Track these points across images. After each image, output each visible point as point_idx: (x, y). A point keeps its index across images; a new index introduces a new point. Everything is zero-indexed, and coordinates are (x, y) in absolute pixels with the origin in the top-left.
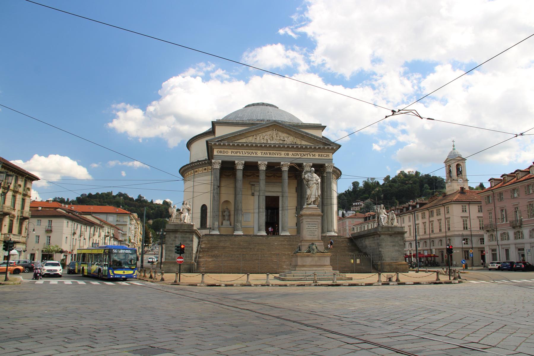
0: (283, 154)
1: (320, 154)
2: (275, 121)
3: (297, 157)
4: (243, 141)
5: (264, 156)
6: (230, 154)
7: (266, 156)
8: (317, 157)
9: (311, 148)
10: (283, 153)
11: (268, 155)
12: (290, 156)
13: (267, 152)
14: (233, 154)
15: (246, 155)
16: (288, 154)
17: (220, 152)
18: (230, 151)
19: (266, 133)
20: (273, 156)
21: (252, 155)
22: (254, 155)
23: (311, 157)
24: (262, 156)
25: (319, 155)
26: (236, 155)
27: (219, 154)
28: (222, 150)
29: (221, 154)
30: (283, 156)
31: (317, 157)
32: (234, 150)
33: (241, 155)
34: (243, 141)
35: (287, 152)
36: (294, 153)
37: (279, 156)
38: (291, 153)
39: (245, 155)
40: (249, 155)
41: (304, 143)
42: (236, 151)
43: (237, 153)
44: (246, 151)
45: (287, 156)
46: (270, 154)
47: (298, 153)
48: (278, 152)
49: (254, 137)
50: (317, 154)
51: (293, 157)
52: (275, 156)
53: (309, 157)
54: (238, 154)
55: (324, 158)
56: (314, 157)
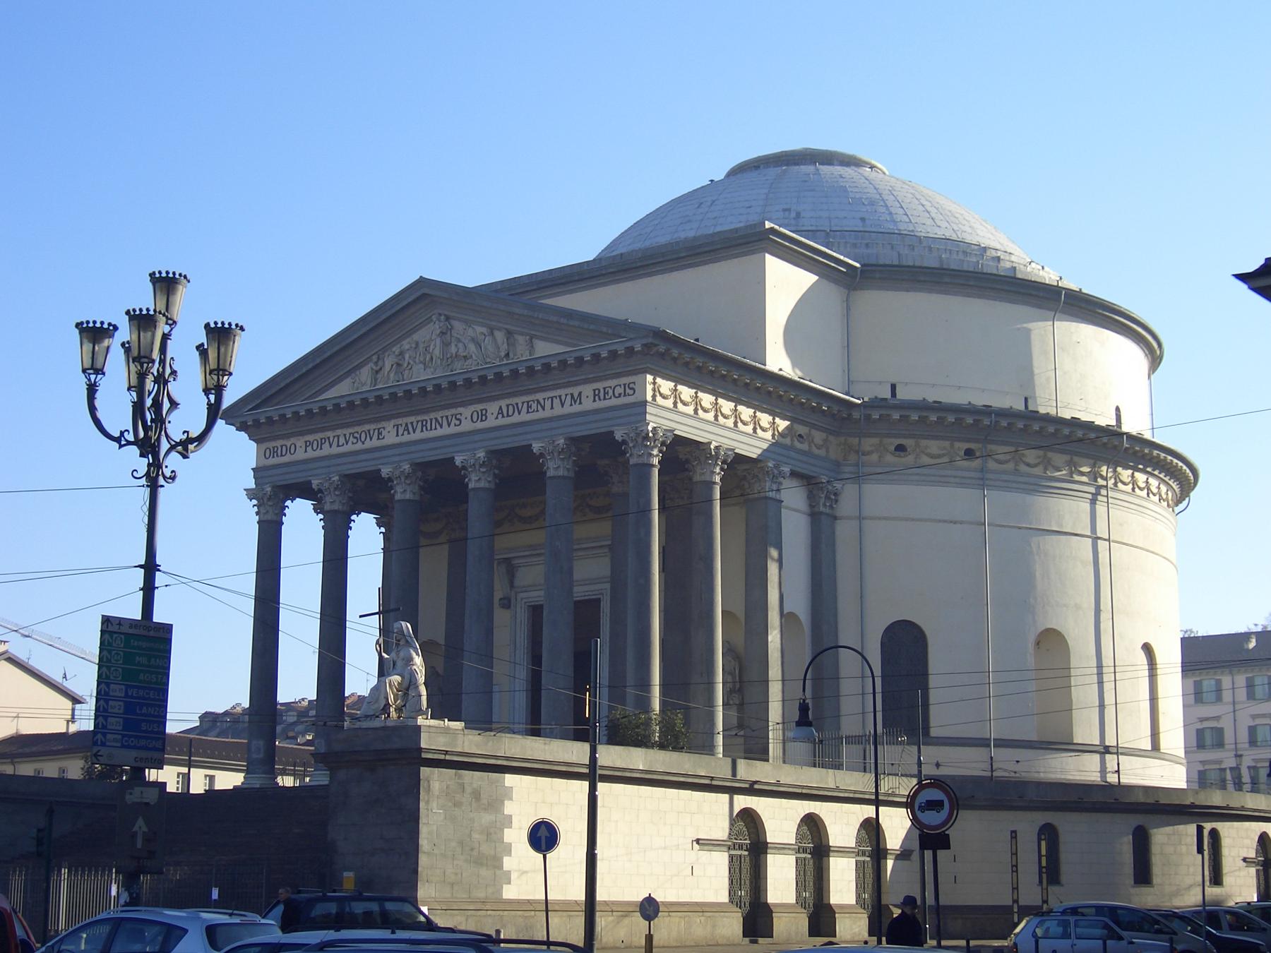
0: (466, 420)
1: (600, 385)
2: (422, 281)
3: (516, 418)
4: (343, 389)
5: (406, 438)
6: (300, 455)
8: (583, 402)
9: (596, 357)
10: (466, 412)
11: (418, 435)
12: (491, 422)
13: (412, 419)
14: (311, 454)
16: (483, 416)
17: (274, 452)
18: (300, 442)
19: (416, 337)
21: (368, 444)
22: (375, 443)
23: (568, 409)
25: (596, 395)
26: (318, 453)
27: (272, 461)
28: (278, 443)
30: (467, 426)
31: (588, 404)
32: (310, 438)
33: (335, 450)
34: (343, 389)
35: (479, 407)
36: (503, 403)
37: (453, 430)
38: (492, 408)
40: (359, 446)
41: (544, 349)
42: (319, 436)
44: (347, 431)
45: (480, 425)
47: (519, 400)
48: (449, 413)
49: (371, 365)
50: (587, 390)
51: (502, 421)
52: (440, 432)
53: (558, 410)
54: (326, 450)
56: (577, 408)
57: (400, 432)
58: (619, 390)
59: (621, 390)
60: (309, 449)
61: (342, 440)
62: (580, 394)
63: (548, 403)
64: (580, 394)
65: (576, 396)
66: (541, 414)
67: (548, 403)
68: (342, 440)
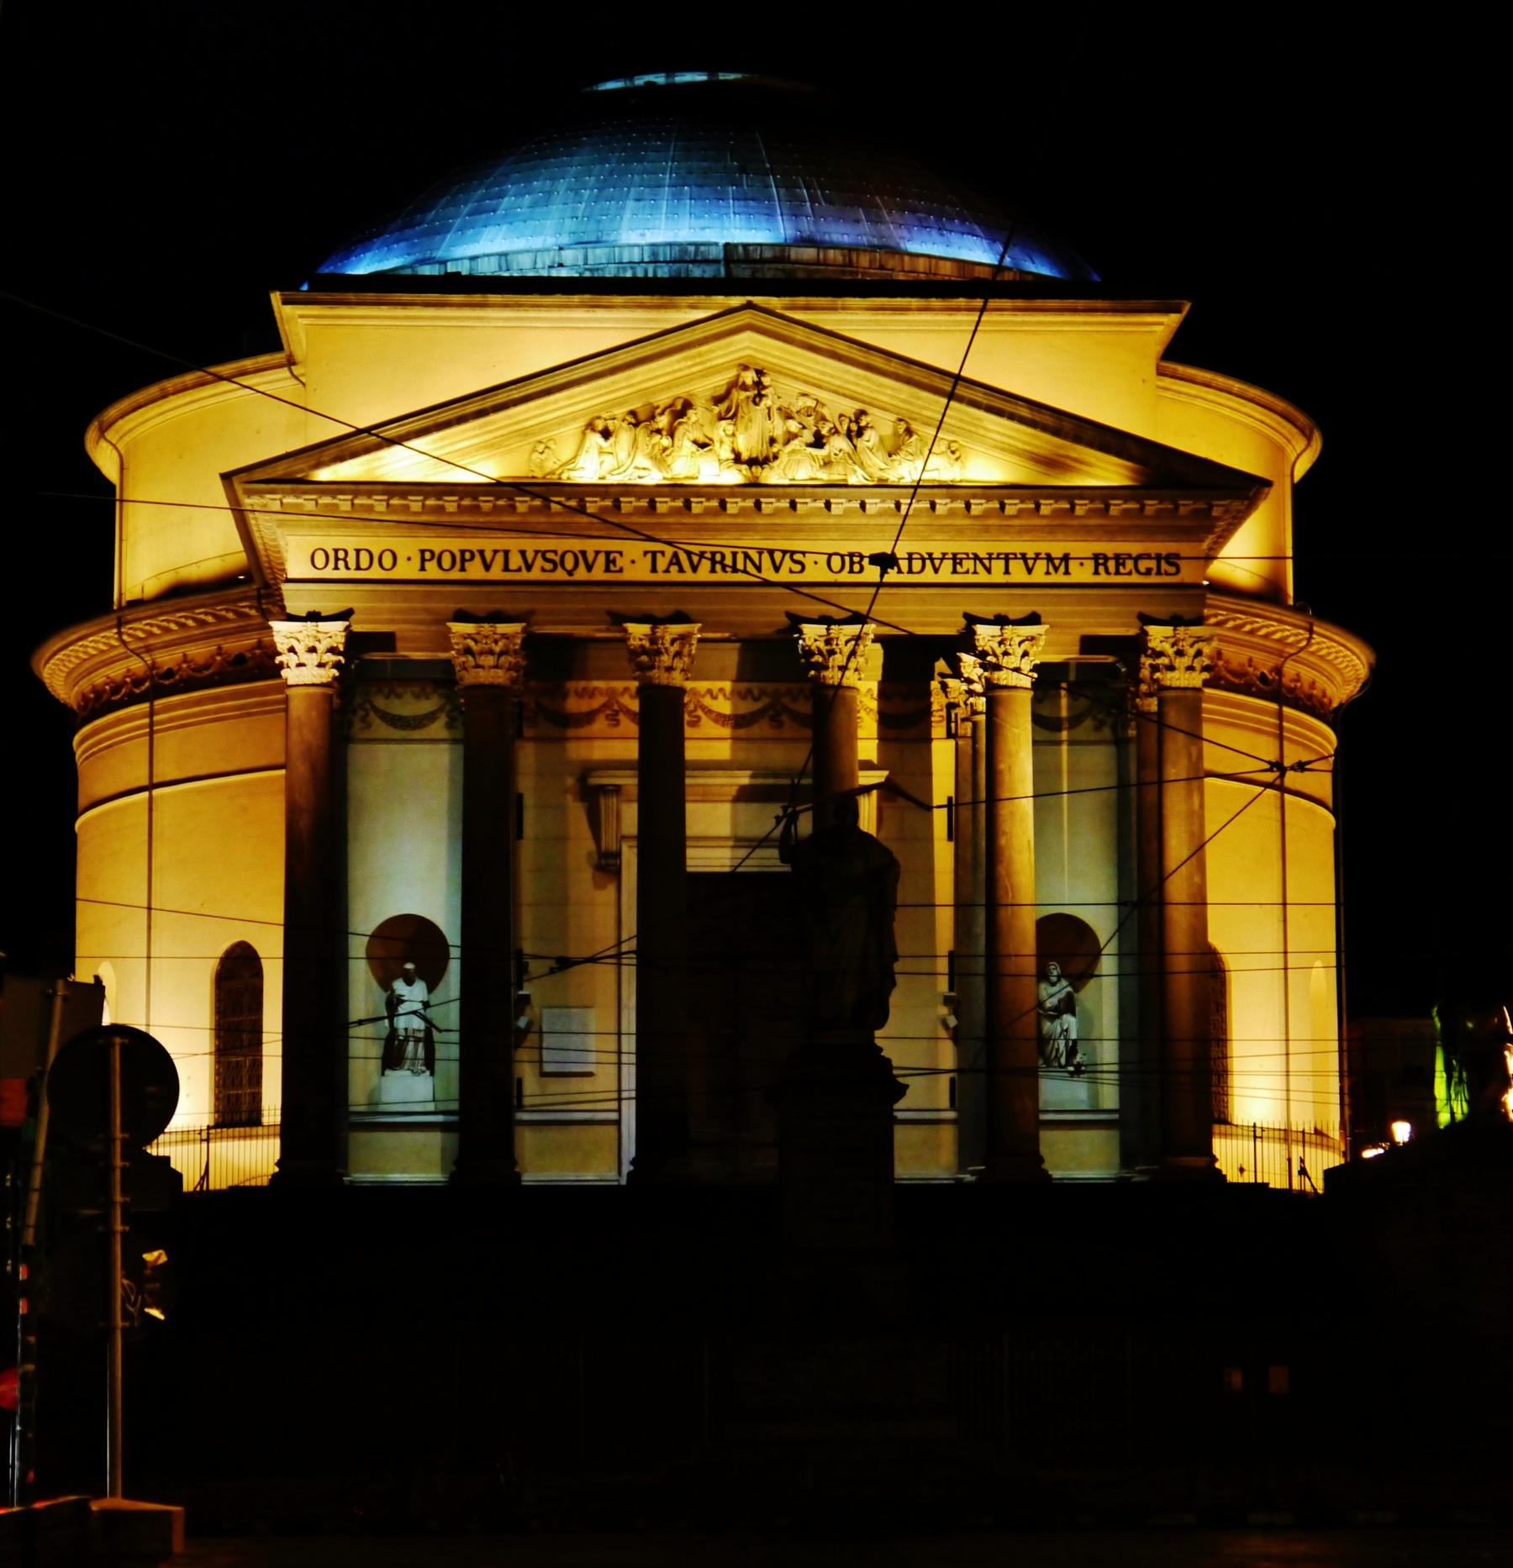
3: (928, 576)
5: (674, 575)
7: (689, 576)
15: (535, 574)
21: (581, 574)
22: (598, 573)
24: (660, 577)
26: (455, 575)
29: (342, 573)
33: (496, 573)
39: (524, 575)
40: (560, 575)
43: (464, 558)
45: (845, 577)
54: (475, 571)
55: (1135, 578)
57: (662, 563)
61: (516, 561)
63: (998, 566)
66: (983, 577)
67: (998, 566)
68: (516, 561)
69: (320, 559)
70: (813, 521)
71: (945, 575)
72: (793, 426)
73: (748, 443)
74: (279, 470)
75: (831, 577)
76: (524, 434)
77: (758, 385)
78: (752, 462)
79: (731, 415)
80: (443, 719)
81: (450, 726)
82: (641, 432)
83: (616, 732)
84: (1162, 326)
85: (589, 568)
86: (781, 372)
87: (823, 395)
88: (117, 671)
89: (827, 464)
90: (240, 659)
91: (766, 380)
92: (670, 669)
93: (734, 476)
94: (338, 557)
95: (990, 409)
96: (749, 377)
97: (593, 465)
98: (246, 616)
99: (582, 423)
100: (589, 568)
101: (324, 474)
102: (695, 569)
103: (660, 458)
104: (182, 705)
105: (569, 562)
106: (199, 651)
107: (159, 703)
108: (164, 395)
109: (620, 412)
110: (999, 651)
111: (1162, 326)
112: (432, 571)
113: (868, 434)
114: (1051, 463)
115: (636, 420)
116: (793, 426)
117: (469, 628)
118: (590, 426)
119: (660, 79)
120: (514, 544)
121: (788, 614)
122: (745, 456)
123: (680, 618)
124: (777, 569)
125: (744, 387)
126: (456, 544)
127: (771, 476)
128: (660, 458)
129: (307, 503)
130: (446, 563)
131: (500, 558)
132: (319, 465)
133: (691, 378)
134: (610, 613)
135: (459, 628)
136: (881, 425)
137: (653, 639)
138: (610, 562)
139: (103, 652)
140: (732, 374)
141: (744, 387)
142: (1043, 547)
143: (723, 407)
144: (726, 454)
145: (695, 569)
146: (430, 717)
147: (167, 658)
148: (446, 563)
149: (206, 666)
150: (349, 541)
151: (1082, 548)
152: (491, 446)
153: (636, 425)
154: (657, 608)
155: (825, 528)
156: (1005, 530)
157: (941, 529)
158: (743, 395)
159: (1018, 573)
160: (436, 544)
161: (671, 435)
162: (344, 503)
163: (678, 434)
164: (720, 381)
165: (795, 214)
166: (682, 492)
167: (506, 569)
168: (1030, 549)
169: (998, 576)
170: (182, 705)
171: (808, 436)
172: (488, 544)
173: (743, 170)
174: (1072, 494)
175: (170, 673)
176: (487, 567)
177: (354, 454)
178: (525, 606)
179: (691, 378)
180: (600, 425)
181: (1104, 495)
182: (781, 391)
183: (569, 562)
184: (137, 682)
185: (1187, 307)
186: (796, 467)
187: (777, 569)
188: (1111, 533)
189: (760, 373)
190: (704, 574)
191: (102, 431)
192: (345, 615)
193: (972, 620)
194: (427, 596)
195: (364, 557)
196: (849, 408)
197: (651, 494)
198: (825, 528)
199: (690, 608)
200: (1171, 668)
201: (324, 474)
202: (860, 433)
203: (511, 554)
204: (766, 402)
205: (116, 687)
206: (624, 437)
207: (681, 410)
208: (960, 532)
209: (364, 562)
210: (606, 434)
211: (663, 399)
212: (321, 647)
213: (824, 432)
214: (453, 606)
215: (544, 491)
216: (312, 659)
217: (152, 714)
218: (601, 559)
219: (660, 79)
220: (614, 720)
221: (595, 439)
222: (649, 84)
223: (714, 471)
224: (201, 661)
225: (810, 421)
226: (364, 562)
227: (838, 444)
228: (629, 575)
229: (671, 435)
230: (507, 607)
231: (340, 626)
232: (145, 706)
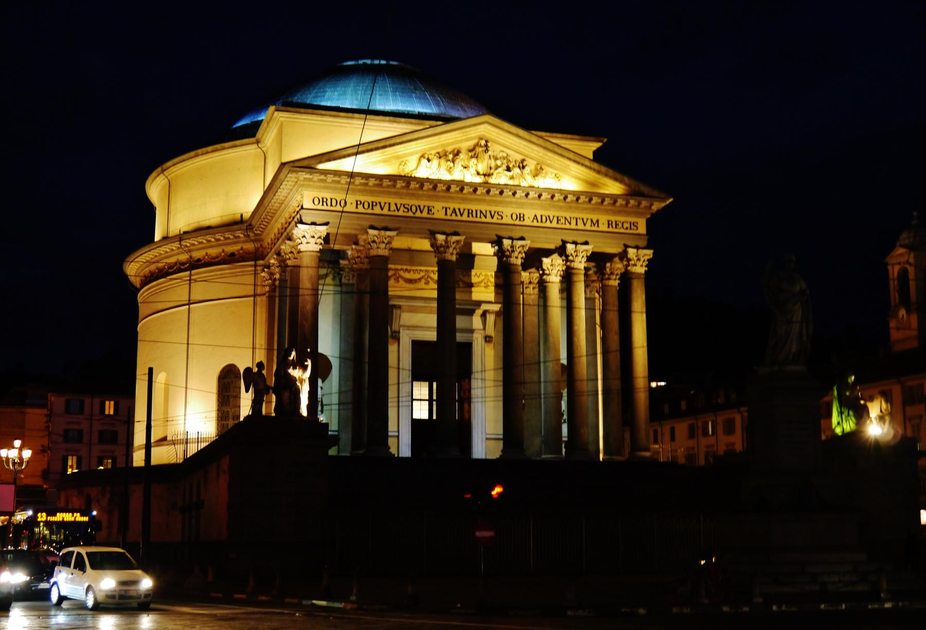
3: (548, 224)
5: (454, 217)
7: (459, 218)
15: (401, 213)
20: (478, 220)
21: (418, 214)
22: (425, 214)
24: (448, 217)
25: (609, 223)
26: (370, 211)
29: (325, 207)
33: (385, 211)
39: (396, 213)
40: (410, 214)
43: (372, 205)
45: (517, 222)
46: (470, 213)
51: (535, 223)
52: (483, 220)
54: (377, 210)
55: (622, 231)
57: (449, 212)
58: (625, 225)
59: (628, 225)
60: (360, 207)
61: (393, 207)
62: (598, 221)
63: (574, 222)
64: (598, 221)
65: (595, 221)
66: (568, 226)
68: (393, 207)
69: (316, 201)
70: (508, 199)
71: (554, 224)
72: (499, 162)
73: (482, 168)
74: (305, 163)
75: (511, 222)
76: (398, 157)
77: (486, 146)
78: (485, 175)
79: (476, 156)
80: (331, 276)
81: (334, 279)
82: (443, 161)
83: (398, 285)
84: (589, 148)
85: (421, 212)
86: (495, 142)
87: (510, 152)
88: (173, 260)
89: (512, 178)
90: (233, 254)
91: (489, 144)
92: (452, 254)
93: (479, 180)
94: (323, 201)
95: (575, 161)
96: (483, 143)
97: (426, 171)
98: (239, 237)
99: (418, 155)
100: (421, 212)
101: (321, 166)
102: (461, 215)
103: (450, 170)
104: (205, 272)
105: (414, 209)
106: (213, 252)
107: (193, 272)
108: (197, 156)
109: (434, 152)
110: (574, 254)
111: (589, 148)
112: (360, 209)
113: (527, 168)
114: (593, 184)
115: (441, 156)
116: (499, 162)
117: (375, 232)
118: (423, 156)
119: (369, 62)
120: (393, 201)
121: (497, 236)
122: (481, 172)
123: (456, 234)
124: (492, 217)
125: (481, 146)
126: (370, 199)
127: (492, 180)
128: (450, 170)
129: (316, 177)
130: (366, 205)
131: (387, 206)
132: (320, 162)
133: (461, 141)
134: (429, 230)
135: (371, 232)
136: (531, 165)
137: (446, 242)
138: (429, 210)
139: (167, 252)
140: (476, 141)
141: (481, 146)
142: (590, 216)
143: (473, 153)
144: (473, 171)
145: (461, 215)
146: (326, 275)
147: (197, 255)
148: (366, 205)
149: (217, 257)
150: (328, 195)
151: (603, 219)
152: (385, 161)
153: (440, 158)
154: (448, 230)
155: (511, 203)
156: (577, 209)
157: (554, 206)
158: (481, 149)
159: (581, 226)
160: (363, 199)
161: (453, 162)
162: (330, 178)
163: (456, 162)
164: (471, 144)
165: (438, 105)
166: (461, 185)
167: (389, 210)
168: (585, 216)
169: (573, 226)
170: (205, 272)
171: (504, 167)
172: (383, 200)
173: (415, 89)
174: (603, 197)
175: (199, 260)
176: (382, 209)
177: (335, 159)
178: (397, 225)
179: (461, 141)
180: (426, 156)
181: (614, 198)
182: (494, 149)
183: (414, 209)
184: (183, 264)
185: (605, 140)
186: (500, 178)
187: (492, 217)
188: (615, 213)
189: (487, 141)
190: (465, 218)
191: (163, 171)
192: (326, 224)
193: (564, 243)
194: (358, 219)
195: (334, 203)
196: (519, 157)
197: (448, 185)
198: (511, 203)
199: (460, 230)
200: (635, 265)
201: (321, 166)
202: (523, 167)
203: (392, 203)
204: (490, 153)
205: (171, 267)
206: (435, 162)
207: (457, 153)
208: (561, 208)
209: (334, 203)
210: (429, 160)
211: (450, 149)
212: (316, 237)
213: (511, 166)
214: (369, 224)
215: (408, 180)
216: (313, 241)
217: (190, 275)
218: (426, 209)
219: (369, 62)
220: (397, 280)
221: (424, 161)
222: (364, 64)
223: (470, 177)
224: (214, 255)
225: (505, 161)
226: (334, 203)
227: (517, 170)
228: (435, 216)
229: (453, 162)
230: (390, 225)
231: (324, 228)
232: (188, 273)
